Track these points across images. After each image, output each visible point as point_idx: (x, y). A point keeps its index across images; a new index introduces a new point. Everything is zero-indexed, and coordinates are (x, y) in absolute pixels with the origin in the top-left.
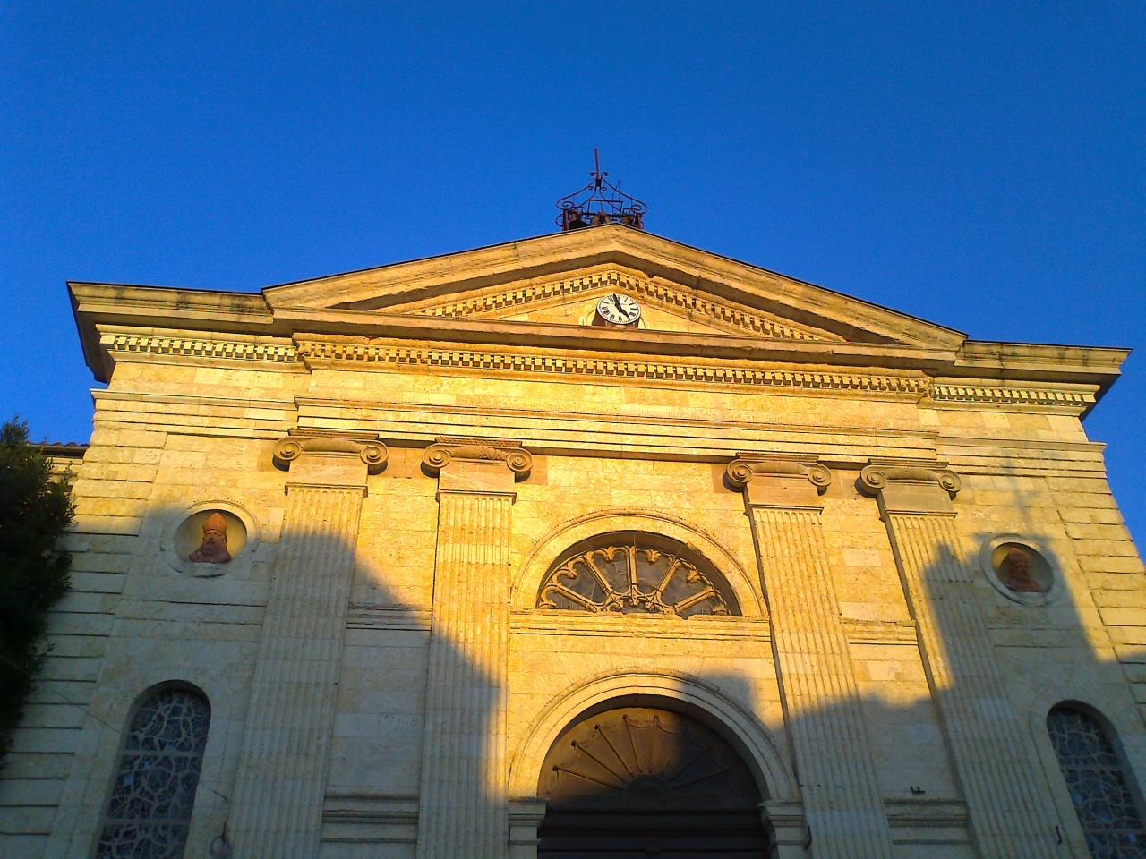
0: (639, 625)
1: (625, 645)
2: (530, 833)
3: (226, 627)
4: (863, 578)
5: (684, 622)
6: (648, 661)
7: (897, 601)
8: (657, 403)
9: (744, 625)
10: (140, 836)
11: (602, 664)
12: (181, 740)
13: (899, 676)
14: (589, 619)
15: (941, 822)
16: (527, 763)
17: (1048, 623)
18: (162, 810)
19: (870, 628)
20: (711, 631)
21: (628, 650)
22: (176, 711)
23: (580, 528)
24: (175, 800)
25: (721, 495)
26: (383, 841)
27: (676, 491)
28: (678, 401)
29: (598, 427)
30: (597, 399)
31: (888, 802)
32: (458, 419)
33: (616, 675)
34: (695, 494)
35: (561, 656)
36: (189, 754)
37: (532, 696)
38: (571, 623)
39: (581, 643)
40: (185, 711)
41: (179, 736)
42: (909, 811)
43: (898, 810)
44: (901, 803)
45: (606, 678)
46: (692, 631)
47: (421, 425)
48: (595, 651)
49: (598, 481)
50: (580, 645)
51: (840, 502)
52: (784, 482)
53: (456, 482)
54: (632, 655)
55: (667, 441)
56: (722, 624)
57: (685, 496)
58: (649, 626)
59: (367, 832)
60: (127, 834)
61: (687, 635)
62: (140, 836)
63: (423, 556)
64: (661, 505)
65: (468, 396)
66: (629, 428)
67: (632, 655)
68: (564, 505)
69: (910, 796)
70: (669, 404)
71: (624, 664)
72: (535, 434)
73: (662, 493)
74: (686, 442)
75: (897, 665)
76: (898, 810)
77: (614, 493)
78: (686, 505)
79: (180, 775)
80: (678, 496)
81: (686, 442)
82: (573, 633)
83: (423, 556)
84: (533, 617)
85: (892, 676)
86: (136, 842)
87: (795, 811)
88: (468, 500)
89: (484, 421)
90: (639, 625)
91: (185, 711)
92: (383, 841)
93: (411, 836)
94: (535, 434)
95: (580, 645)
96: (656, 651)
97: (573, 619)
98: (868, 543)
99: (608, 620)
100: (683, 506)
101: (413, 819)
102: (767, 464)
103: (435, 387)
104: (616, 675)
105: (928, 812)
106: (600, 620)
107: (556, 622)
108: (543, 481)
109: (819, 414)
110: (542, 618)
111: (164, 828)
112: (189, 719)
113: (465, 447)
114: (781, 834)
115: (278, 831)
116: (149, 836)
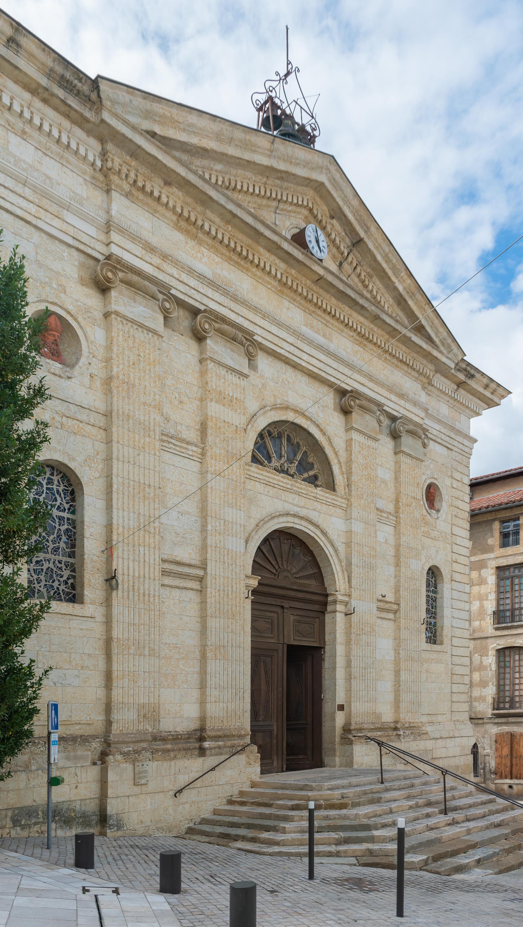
0: (298, 487)
1: (290, 497)
3: (81, 425)
4: (383, 485)
8: (318, 332)
10: (46, 565)
11: (280, 506)
12: (58, 503)
17: (436, 527)
18: (56, 550)
20: (325, 499)
21: (291, 501)
22: (50, 481)
24: (62, 545)
26: (186, 588)
33: (288, 514)
36: (66, 515)
38: (268, 477)
39: (273, 491)
40: (56, 482)
41: (56, 500)
46: (318, 496)
48: (277, 498)
50: (271, 492)
54: (292, 504)
58: (301, 489)
59: (177, 582)
60: (37, 562)
62: (46, 565)
63: (194, 404)
67: (292, 504)
68: (266, 392)
70: (324, 336)
74: (330, 371)
75: (387, 535)
79: (63, 528)
81: (330, 371)
82: (267, 484)
83: (194, 404)
86: (45, 568)
90: (298, 487)
91: (56, 482)
92: (186, 588)
93: (198, 587)
99: (285, 481)
104: (288, 514)
106: (282, 479)
107: (262, 475)
111: (60, 562)
112: (60, 489)
115: (139, 577)
116: (51, 565)
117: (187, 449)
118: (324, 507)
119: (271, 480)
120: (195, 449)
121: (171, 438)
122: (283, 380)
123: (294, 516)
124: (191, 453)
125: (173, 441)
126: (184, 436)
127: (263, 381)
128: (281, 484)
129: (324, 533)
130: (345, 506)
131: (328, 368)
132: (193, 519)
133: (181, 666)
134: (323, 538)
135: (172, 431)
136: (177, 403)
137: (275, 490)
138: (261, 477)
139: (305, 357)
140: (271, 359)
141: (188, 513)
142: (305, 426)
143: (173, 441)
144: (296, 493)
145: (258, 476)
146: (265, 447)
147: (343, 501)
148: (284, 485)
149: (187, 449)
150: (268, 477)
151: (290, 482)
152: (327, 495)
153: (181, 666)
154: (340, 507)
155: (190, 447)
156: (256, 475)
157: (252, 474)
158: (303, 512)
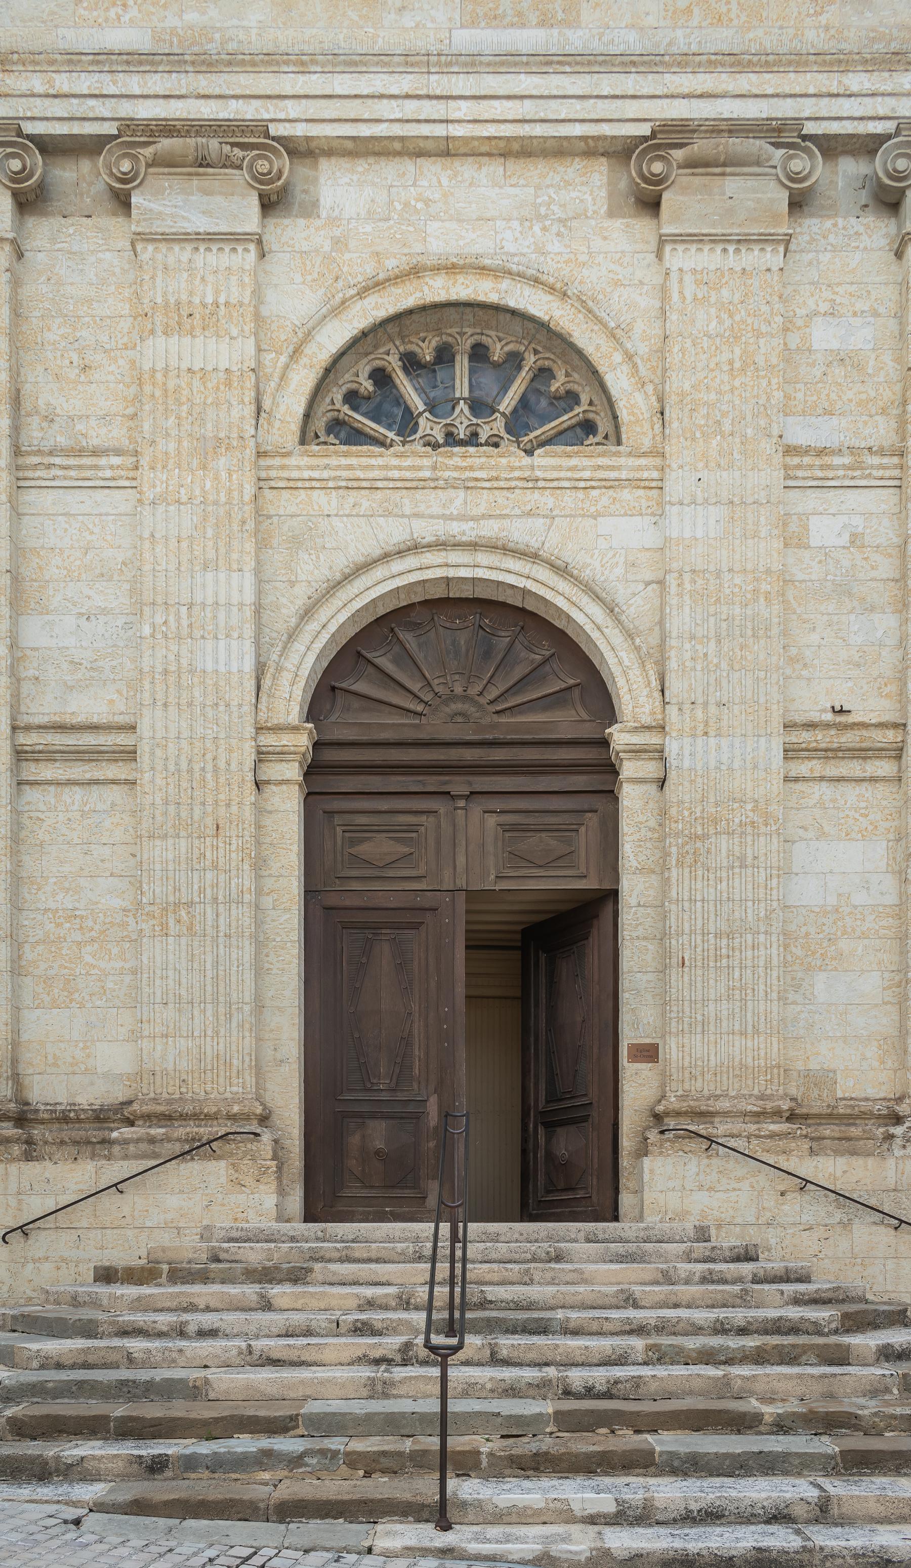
0: (457, 468)
1: (432, 502)
2: (293, 771)
5: (527, 460)
6: (467, 526)
7: (884, 412)
9: (622, 461)
13: (855, 539)
14: (380, 461)
15: (862, 753)
16: (286, 678)
19: (827, 460)
20: (569, 474)
21: (436, 510)
23: (371, 300)
25: (619, 223)
26: (96, 782)
27: (540, 218)
28: (560, 15)
29: (405, 84)
30: (408, 21)
31: (788, 726)
32: (157, 83)
33: (415, 548)
34: (575, 224)
35: (335, 521)
37: (292, 584)
38: (350, 467)
39: (366, 501)
42: (821, 738)
43: (804, 737)
44: (811, 726)
45: (401, 553)
46: (539, 474)
47: (92, 102)
48: (388, 514)
49: (406, 204)
50: (365, 504)
51: (828, 224)
52: (732, 185)
53: (160, 216)
54: (444, 517)
55: (527, 109)
56: (586, 462)
57: (555, 229)
58: (471, 468)
59: (78, 771)
61: (533, 483)
63: (121, 362)
64: (510, 247)
65: (173, 31)
66: (461, 84)
67: (444, 517)
68: (347, 256)
69: (829, 717)
70: (543, 23)
71: (425, 531)
72: (293, 109)
73: (515, 224)
74: (562, 110)
76: (804, 737)
77: (433, 227)
78: (555, 246)
80: (544, 229)
81: (562, 110)
82: (352, 486)
83: (121, 362)
84: (292, 461)
85: (845, 539)
87: (653, 739)
88: (182, 253)
89: (203, 83)
90: (457, 468)
92: (96, 782)
94: (293, 109)
95: (365, 504)
96: (481, 510)
97: (353, 461)
98: (860, 306)
99: (408, 462)
100: (549, 248)
101: (130, 755)
102: (700, 146)
103: (112, 14)
105: (849, 739)
106: (395, 462)
107: (327, 467)
108: (310, 210)
109: (827, 28)
110: (305, 461)
113: (165, 144)
114: (628, 769)
117: (96, 467)
118: (569, 499)
119: (360, 474)
120: (116, 460)
121: (51, 453)
122: (406, 204)
123: (441, 545)
124: (108, 473)
125: (57, 461)
126: (95, 442)
127: (337, 232)
128: (396, 474)
129: (562, 570)
130: (655, 475)
131: (553, 104)
132: (120, 623)
133: (89, 959)
134: (562, 585)
135: (62, 440)
136: (73, 373)
137: (379, 495)
138: (325, 474)
139: (463, 109)
140: (361, 165)
141: (104, 611)
142: (493, 298)
143: (57, 461)
144: (450, 485)
145: (316, 474)
146: (399, 400)
147: (643, 461)
148: (408, 474)
149: (96, 467)
150: (350, 467)
151: (426, 462)
152: (574, 462)
153: (89, 959)
154: (635, 483)
155: (103, 461)
156: (306, 474)
157: (295, 474)
158: (490, 529)
